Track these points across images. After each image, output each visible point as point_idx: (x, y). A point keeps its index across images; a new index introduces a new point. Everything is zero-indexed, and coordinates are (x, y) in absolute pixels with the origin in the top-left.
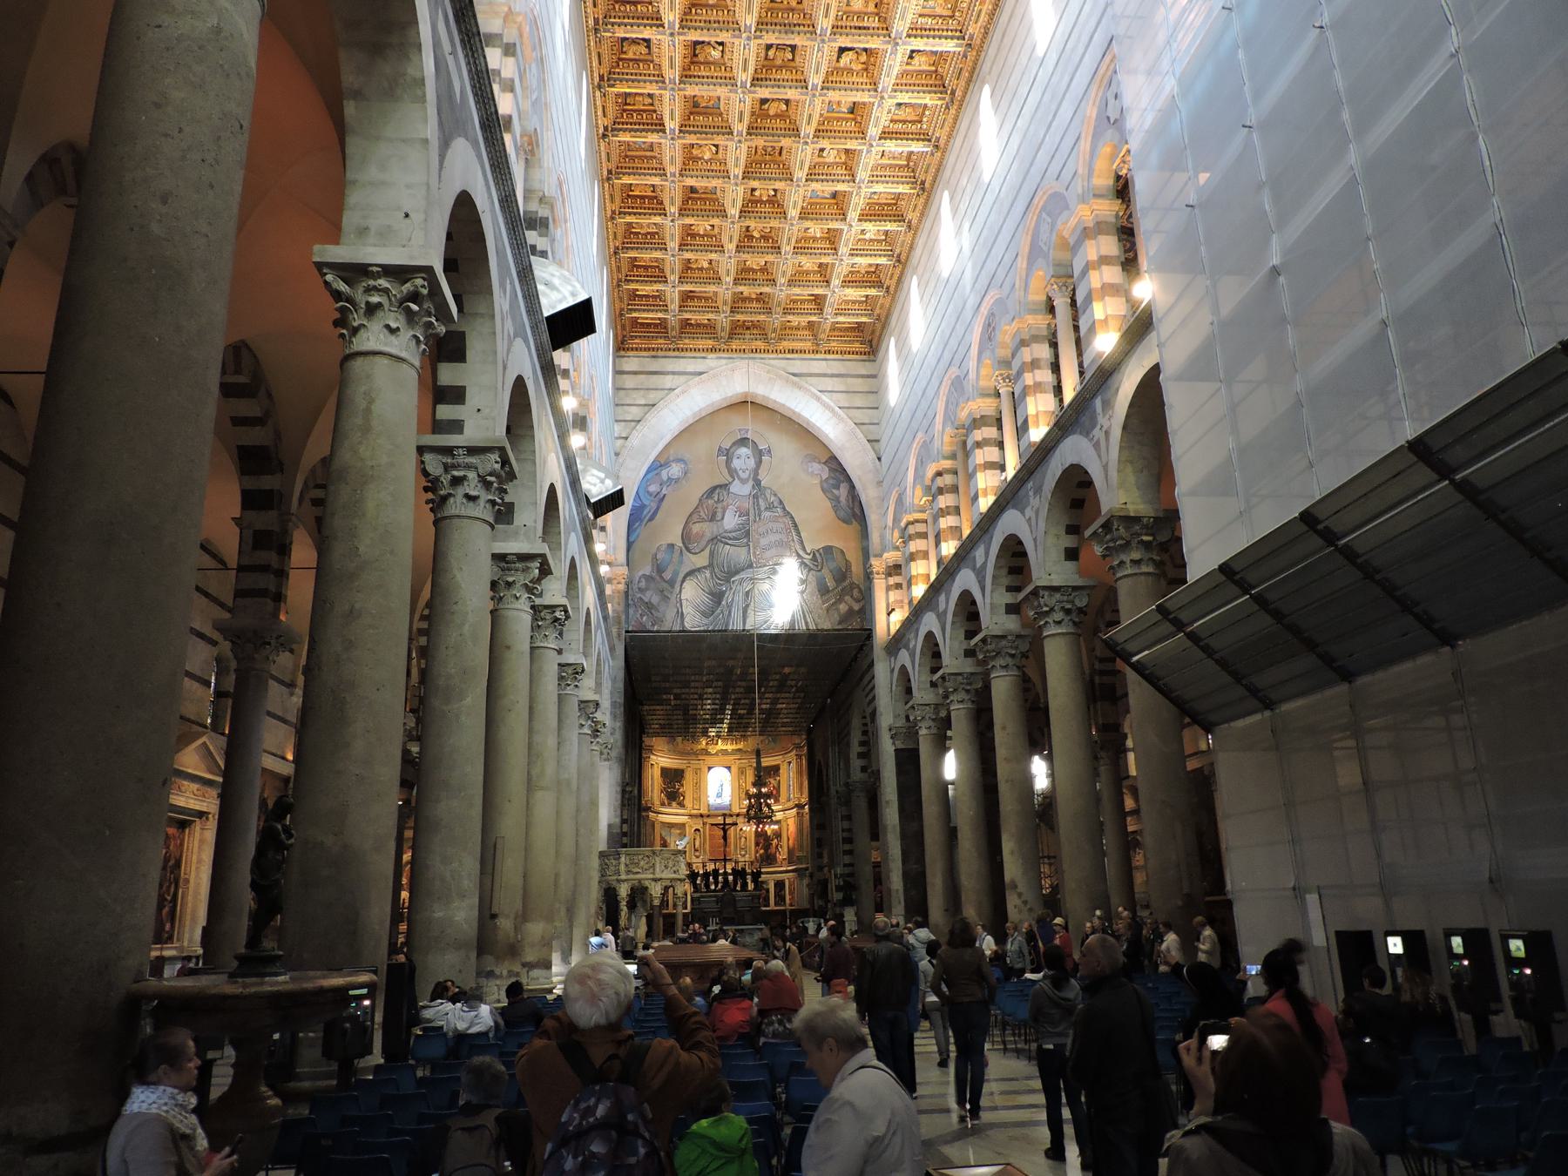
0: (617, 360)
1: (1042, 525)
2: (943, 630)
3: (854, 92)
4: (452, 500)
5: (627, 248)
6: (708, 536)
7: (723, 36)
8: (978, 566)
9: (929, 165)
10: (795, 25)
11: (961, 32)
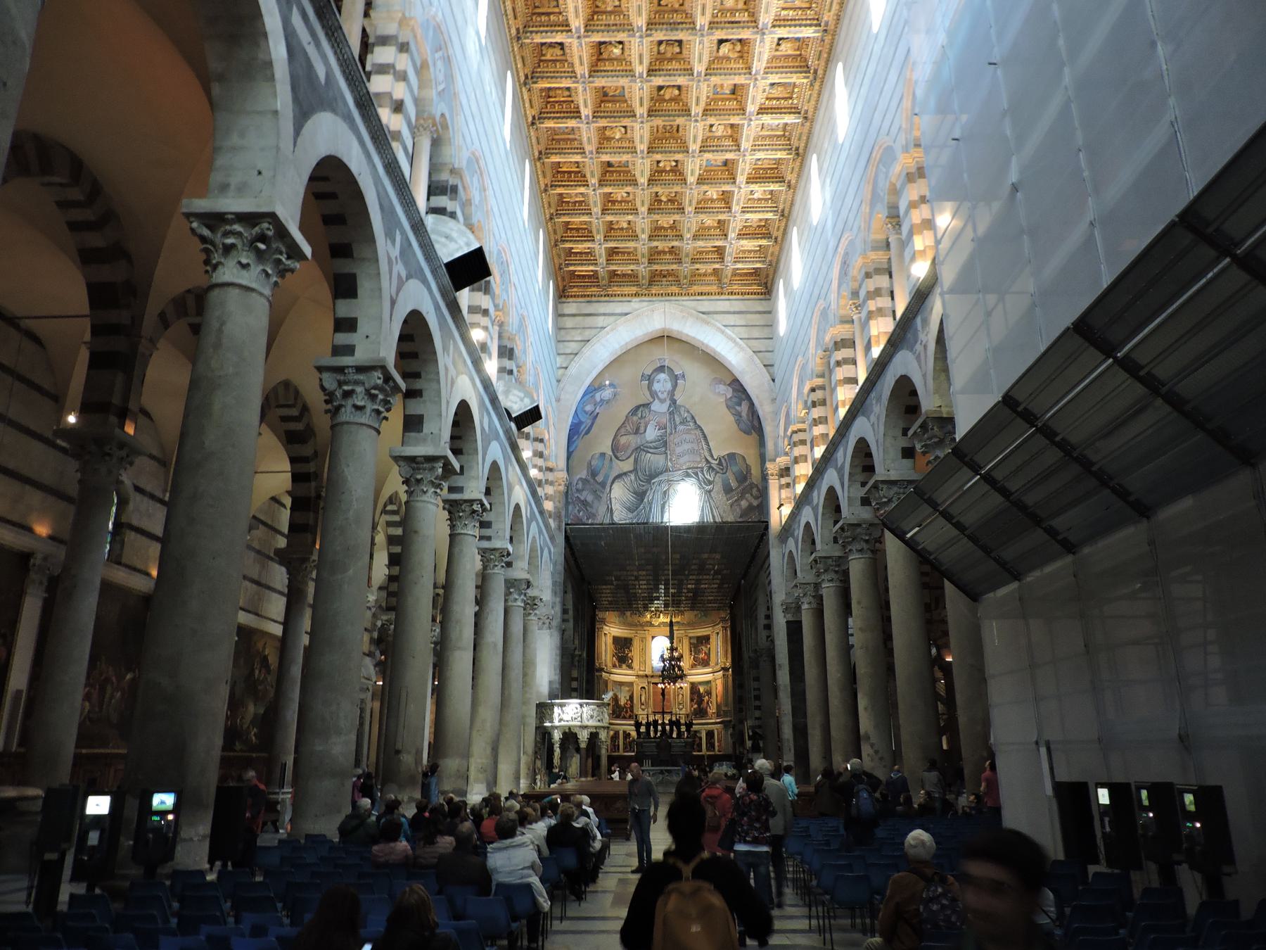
0: (559, 306)
1: (882, 428)
2: (817, 520)
3: (733, 76)
4: (343, 410)
5: (560, 214)
6: (633, 446)
9: (801, 134)
10: (679, 23)
11: (818, 19)
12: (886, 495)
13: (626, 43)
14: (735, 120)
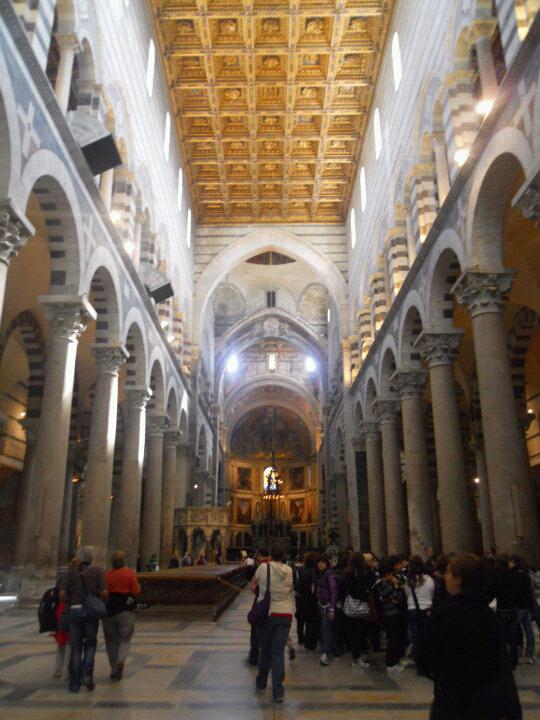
1: (428, 295)
7: (235, 15)
8: (394, 331)
13: (239, 22)
14: (319, 84)
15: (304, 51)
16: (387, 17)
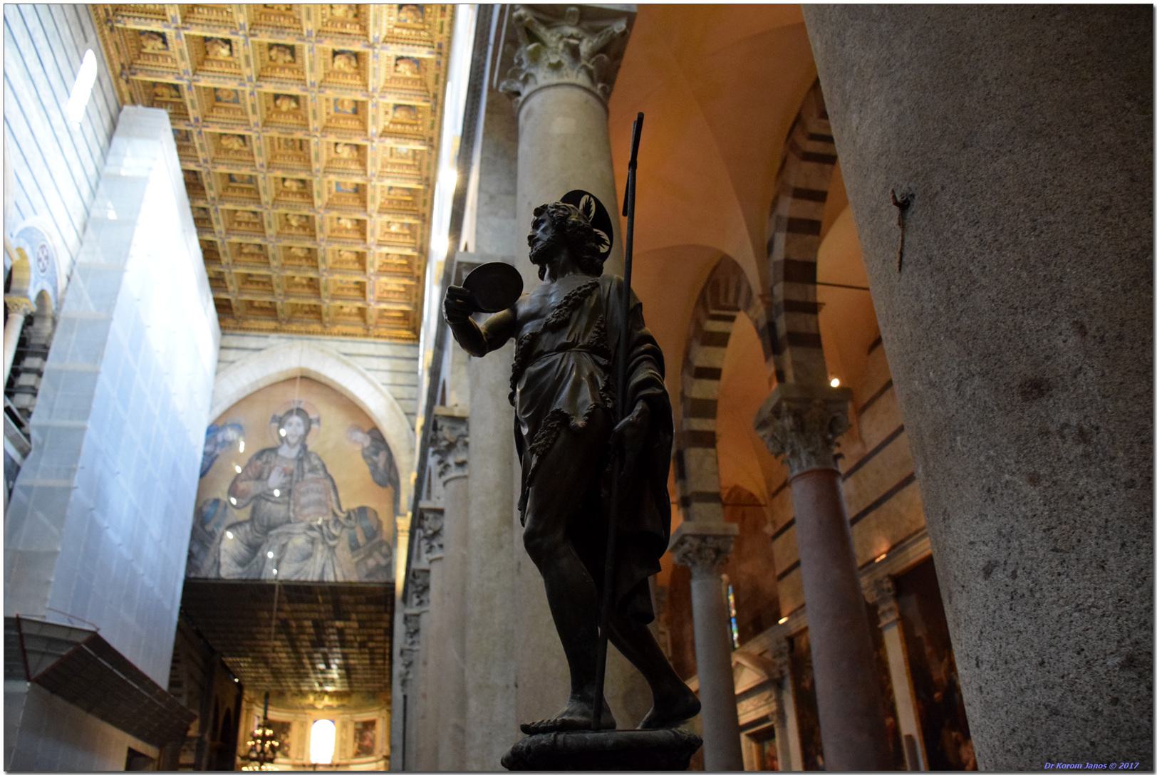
10: (286, 28)
12: (432, 526)
13: (233, 44)
15: (330, 93)
16: (443, 61)
